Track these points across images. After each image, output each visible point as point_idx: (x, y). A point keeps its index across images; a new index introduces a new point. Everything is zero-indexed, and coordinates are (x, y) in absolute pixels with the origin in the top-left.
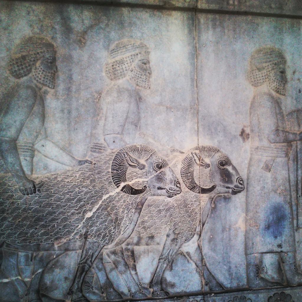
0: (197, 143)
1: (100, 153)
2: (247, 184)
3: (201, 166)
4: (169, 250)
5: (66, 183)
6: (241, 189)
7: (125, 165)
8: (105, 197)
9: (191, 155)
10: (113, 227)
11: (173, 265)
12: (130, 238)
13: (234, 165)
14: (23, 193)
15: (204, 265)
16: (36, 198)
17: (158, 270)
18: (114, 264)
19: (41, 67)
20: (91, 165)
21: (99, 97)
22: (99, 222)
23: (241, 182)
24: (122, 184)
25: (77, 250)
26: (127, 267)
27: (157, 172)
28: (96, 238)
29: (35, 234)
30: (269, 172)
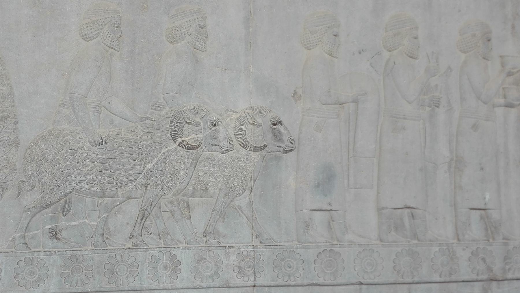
0: (250, 103)
1: (160, 110)
2: (299, 144)
3: (253, 125)
4: (222, 203)
5: (129, 137)
6: (292, 149)
7: (182, 122)
8: (163, 152)
9: (244, 115)
10: (170, 179)
11: (225, 217)
12: (185, 189)
13: (285, 125)
14: (91, 144)
15: (255, 218)
16: (103, 149)
17: (211, 220)
18: (171, 213)
19: (108, 31)
20: (151, 121)
21: (159, 59)
22: (158, 174)
23: (293, 142)
24: (180, 140)
25: (139, 198)
26: (183, 216)
27: (211, 129)
28: (155, 188)
29: (102, 181)
30: (320, 132)
